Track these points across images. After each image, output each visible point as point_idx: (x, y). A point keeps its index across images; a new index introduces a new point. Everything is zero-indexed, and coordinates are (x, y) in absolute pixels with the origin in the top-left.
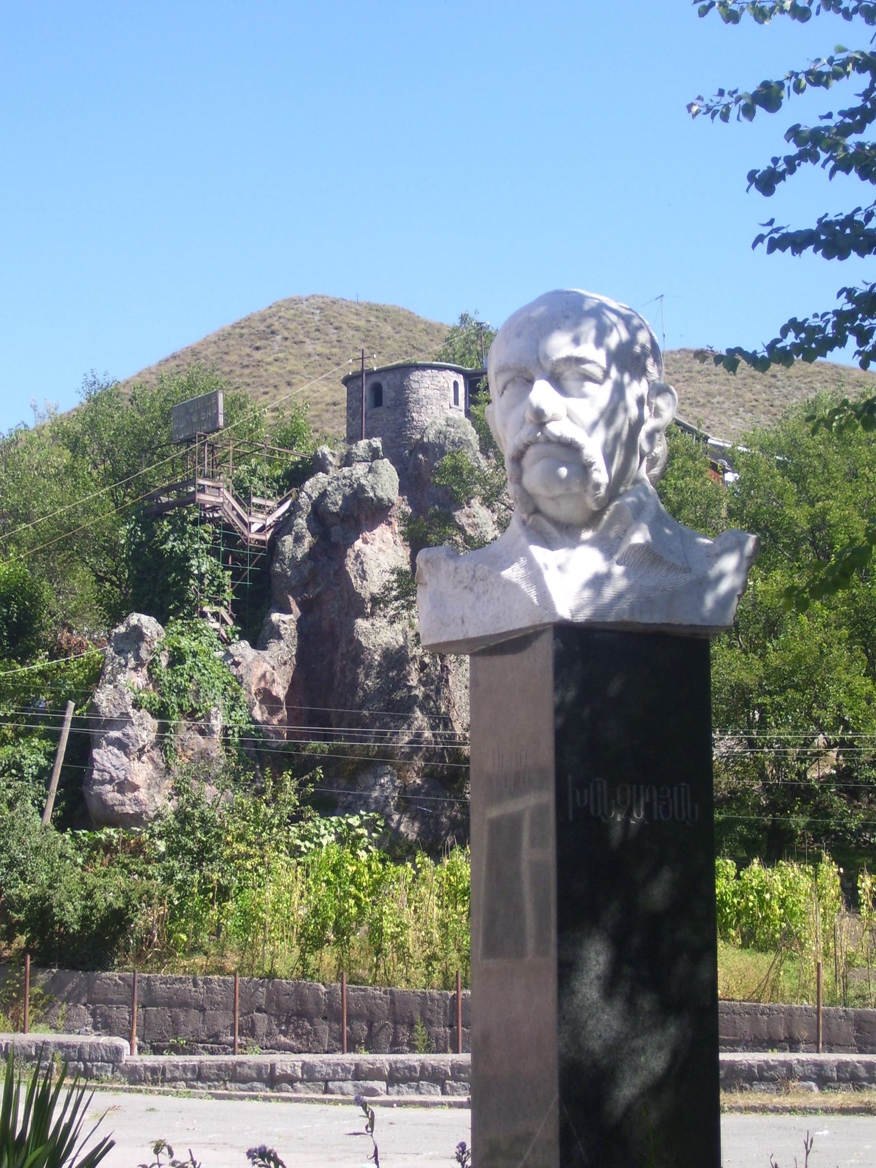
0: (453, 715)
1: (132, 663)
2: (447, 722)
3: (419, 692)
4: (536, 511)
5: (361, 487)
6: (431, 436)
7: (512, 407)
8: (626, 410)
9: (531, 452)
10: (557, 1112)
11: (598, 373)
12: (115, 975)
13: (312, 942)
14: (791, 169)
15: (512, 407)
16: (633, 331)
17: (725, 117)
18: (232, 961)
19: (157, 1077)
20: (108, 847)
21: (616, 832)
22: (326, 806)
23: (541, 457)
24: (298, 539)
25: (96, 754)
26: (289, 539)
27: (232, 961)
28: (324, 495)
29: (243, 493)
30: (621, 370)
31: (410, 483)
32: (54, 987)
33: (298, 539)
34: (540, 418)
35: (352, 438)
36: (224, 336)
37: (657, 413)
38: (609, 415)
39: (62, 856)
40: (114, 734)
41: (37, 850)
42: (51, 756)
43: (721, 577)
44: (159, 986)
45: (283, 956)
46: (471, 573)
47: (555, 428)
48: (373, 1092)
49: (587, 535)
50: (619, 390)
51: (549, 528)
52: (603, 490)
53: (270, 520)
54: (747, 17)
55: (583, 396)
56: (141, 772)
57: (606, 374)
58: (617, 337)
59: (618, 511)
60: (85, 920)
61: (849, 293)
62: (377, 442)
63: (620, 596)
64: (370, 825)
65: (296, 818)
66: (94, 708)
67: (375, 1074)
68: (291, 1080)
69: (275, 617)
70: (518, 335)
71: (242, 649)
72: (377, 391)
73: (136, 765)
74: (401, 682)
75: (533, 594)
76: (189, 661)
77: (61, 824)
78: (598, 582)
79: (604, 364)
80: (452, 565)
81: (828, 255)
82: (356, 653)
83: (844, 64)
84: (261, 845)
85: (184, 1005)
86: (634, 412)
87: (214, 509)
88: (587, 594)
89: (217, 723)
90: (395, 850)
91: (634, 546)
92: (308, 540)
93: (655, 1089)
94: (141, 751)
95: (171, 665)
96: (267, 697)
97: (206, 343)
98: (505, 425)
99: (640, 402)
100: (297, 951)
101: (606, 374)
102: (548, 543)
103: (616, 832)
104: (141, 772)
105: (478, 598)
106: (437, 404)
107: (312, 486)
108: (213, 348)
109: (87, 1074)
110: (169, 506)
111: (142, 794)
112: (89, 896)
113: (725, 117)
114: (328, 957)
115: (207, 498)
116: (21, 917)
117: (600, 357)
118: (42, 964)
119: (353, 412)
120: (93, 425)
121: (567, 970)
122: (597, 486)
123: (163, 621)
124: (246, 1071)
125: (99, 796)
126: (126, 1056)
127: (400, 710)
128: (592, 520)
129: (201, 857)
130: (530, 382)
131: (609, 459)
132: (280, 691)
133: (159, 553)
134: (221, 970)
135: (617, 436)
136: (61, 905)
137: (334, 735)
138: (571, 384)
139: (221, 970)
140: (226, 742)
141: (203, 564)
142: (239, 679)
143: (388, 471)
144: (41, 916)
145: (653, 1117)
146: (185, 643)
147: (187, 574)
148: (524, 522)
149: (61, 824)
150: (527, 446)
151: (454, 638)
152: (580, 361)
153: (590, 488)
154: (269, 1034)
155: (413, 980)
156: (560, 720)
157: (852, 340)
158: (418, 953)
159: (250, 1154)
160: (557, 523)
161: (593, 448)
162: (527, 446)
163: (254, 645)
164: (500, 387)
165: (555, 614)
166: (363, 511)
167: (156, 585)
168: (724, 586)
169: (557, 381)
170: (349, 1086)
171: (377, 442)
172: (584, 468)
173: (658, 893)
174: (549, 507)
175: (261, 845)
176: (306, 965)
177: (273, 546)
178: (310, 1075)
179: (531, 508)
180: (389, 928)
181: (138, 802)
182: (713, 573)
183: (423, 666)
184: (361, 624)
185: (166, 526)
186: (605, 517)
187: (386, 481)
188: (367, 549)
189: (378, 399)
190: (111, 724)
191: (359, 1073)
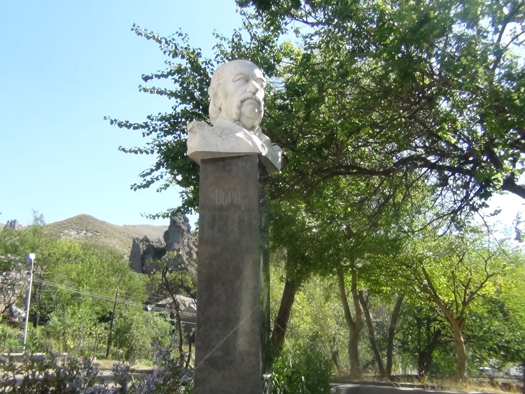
9: (249, 101)
46: (221, 132)
75: (250, 143)
105: (223, 140)
150: (248, 99)
151: (213, 151)
162: (248, 99)
174: (244, 120)
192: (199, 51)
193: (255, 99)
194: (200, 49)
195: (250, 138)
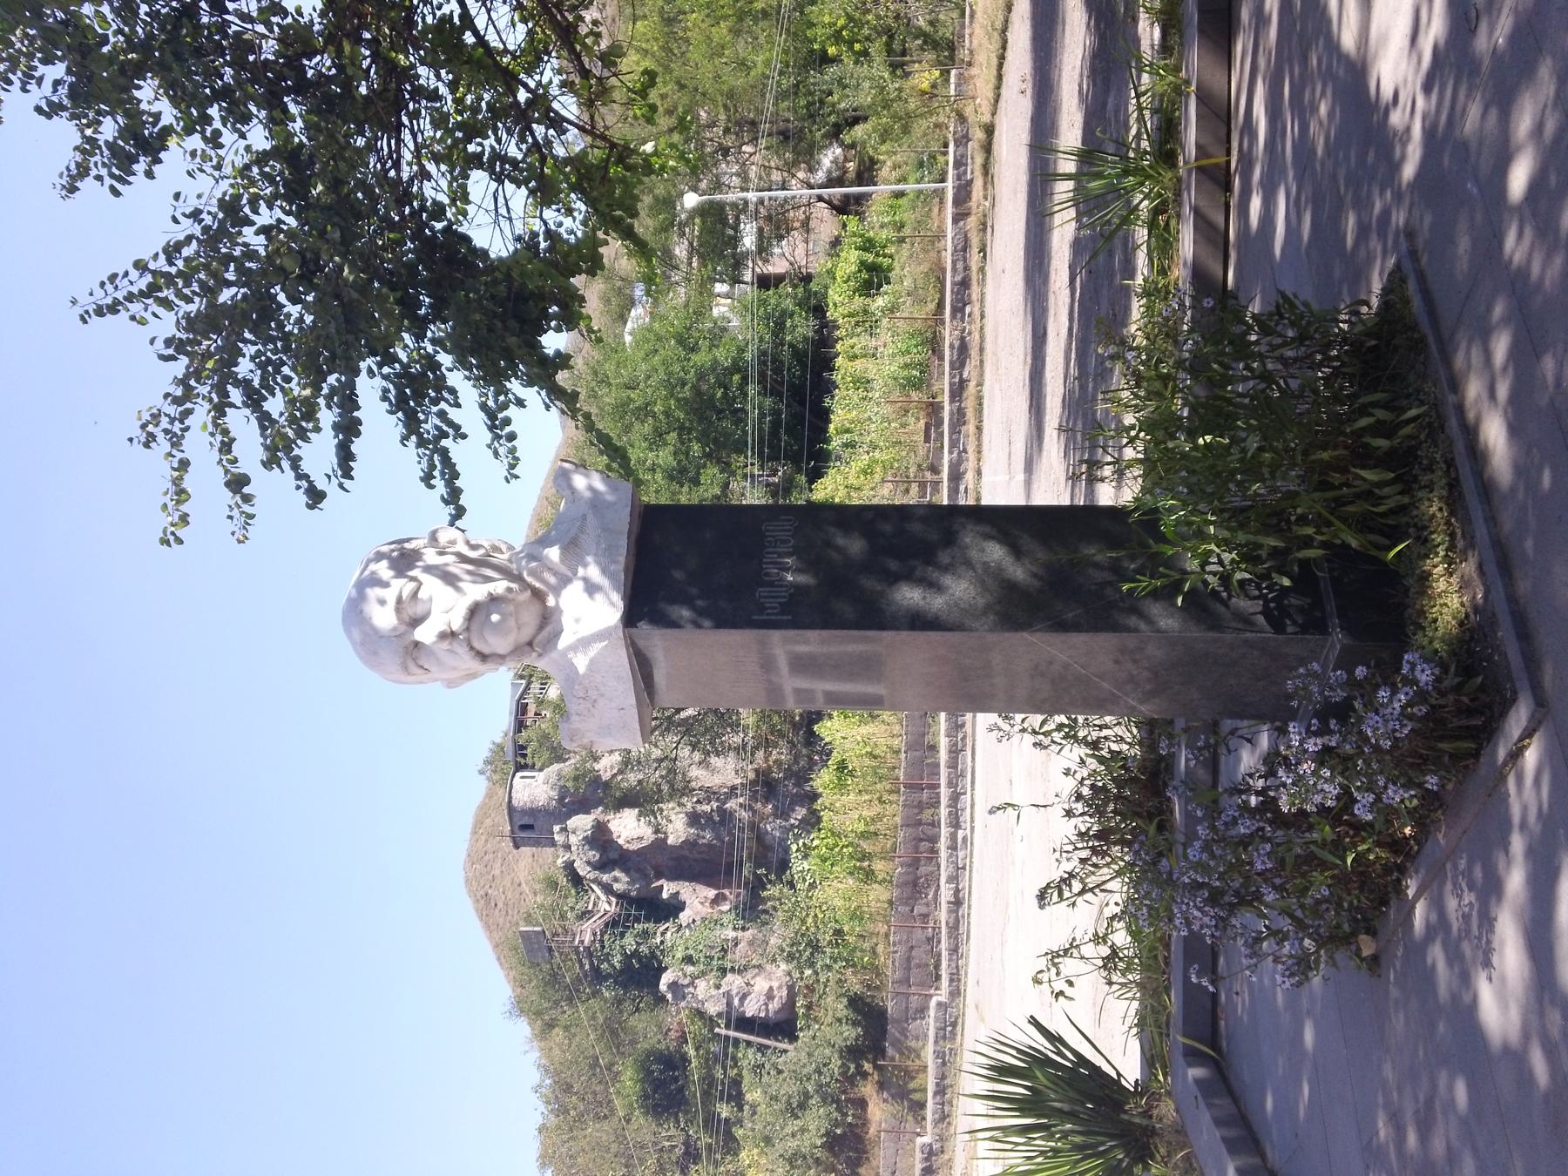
0: (730, 784)
1: (691, 989)
2: (733, 788)
3: (715, 805)
4: (530, 644)
5: (585, 838)
6: (554, 794)
7: (439, 661)
9: (477, 645)
10: (1039, 635)
11: (413, 585)
12: (890, 1005)
13: (869, 875)
14: (306, 477)
15: (439, 661)
16: (379, 556)
17: (252, 517)
18: (882, 928)
19: (955, 978)
20: (809, 1007)
21: (803, 579)
22: (784, 865)
23: (482, 637)
24: (616, 880)
25: (749, 1014)
26: (616, 886)
27: (882, 928)
28: (588, 863)
29: (585, 915)
30: (411, 567)
31: (583, 806)
32: (897, 1044)
33: (616, 880)
34: (448, 635)
35: (553, 844)
36: (487, 926)
37: (453, 542)
38: (450, 579)
39: (814, 1038)
40: (736, 1002)
41: (810, 1055)
42: (749, 1044)
43: (591, 488)
44: (898, 975)
45: (878, 895)
47: (457, 623)
48: (965, 839)
49: (551, 601)
51: (545, 633)
52: (514, 586)
53: (603, 897)
54: (184, 508)
55: (431, 599)
56: (761, 985)
57: (413, 579)
58: (383, 570)
59: (532, 573)
60: (855, 1024)
61: (404, 439)
62: (557, 828)
63: (604, 571)
64: (797, 837)
65: (792, 885)
66: (719, 1015)
67: (953, 837)
68: (957, 891)
69: (665, 895)
70: (375, 653)
71: (684, 917)
72: (524, 827)
73: (756, 988)
74: (708, 816)
75: (599, 646)
76: (691, 952)
77: (793, 1038)
78: (591, 588)
79: (404, 581)
80: (574, 718)
81: (358, 434)
82: (689, 844)
83: (216, 425)
84: (809, 908)
85: (909, 959)
86: (450, 559)
87: (595, 934)
88: (599, 597)
89: (731, 934)
90: (812, 822)
91: (562, 561)
92: (617, 873)
93: (1017, 552)
94: (748, 984)
95: (693, 964)
96: (716, 901)
97: (490, 938)
98: (455, 668)
99: (441, 554)
100: (875, 886)
101: (413, 579)
102: (558, 634)
103: (803, 579)
104: (761, 985)
106: (535, 789)
107: (583, 870)
108: (495, 934)
109: (954, 1024)
110: (592, 963)
111: (775, 985)
112: (839, 1020)
113: (252, 517)
114: (879, 866)
115: (587, 939)
116: (852, 1067)
118: (882, 1052)
119: (537, 843)
120: (538, 1014)
121: (920, 622)
122: (509, 590)
123: (666, 968)
124: (952, 920)
125: (776, 1013)
126: (943, 999)
127: (726, 817)
128: (538, 596)
129: (815, 947)
130: (417, 644)
131: (488, 579)
132: (712, 893)
133: (622, 972)
134: (887, 935)
135: (469, 572)
136: (845, 1040)
137: (740, 861)
138: (420, 609)
139: (887, 935)
140: (743, 929)
141: (629, 942)
142: (704, 919)
143: (573, 822)
144: (853, 1053)
145: (1042, 554)
146: (679, 955)
147: (635, 954)
148: (540, 655)
149: (793, 1038)
150: (472, 648)
152: (399, 601)
153: (510, 596)
154: (927, 905)
155: (895, 812)
156: (707, 623)
157: (444, 443)
158: (877, 809)
159: (1042, 907)
160: (541, 627)
161: (477, 592)
162: (472, 648)
163: (683, 909)
164: (420, 671)
165: (616, 627)
166: (600, 838)
167: (641, 975)
168: (599, 485)
169: (416, 622)
170: (961, 854)
171: (557, 828)
172: (493, 599)
173: (855, 546)
174: (527, 633)
175: (809, 908)
176: (884, 880)
177: (620, 896)
178: (954, 879)
179: (528, 648)
180: (861, 827)
181: (780, 987)
182: (588, 494)
183: (699, 802)
184: (669, 842)
185: (604, 966)
186: (538, 585)
187: (582, 823)
188: (623, 836)
189: (529, 827)
190: (729, 1004)
191: (953, 847)
192: (159, 344)
193: (468, 629)
194: (152, 342)
195: (583, 643)
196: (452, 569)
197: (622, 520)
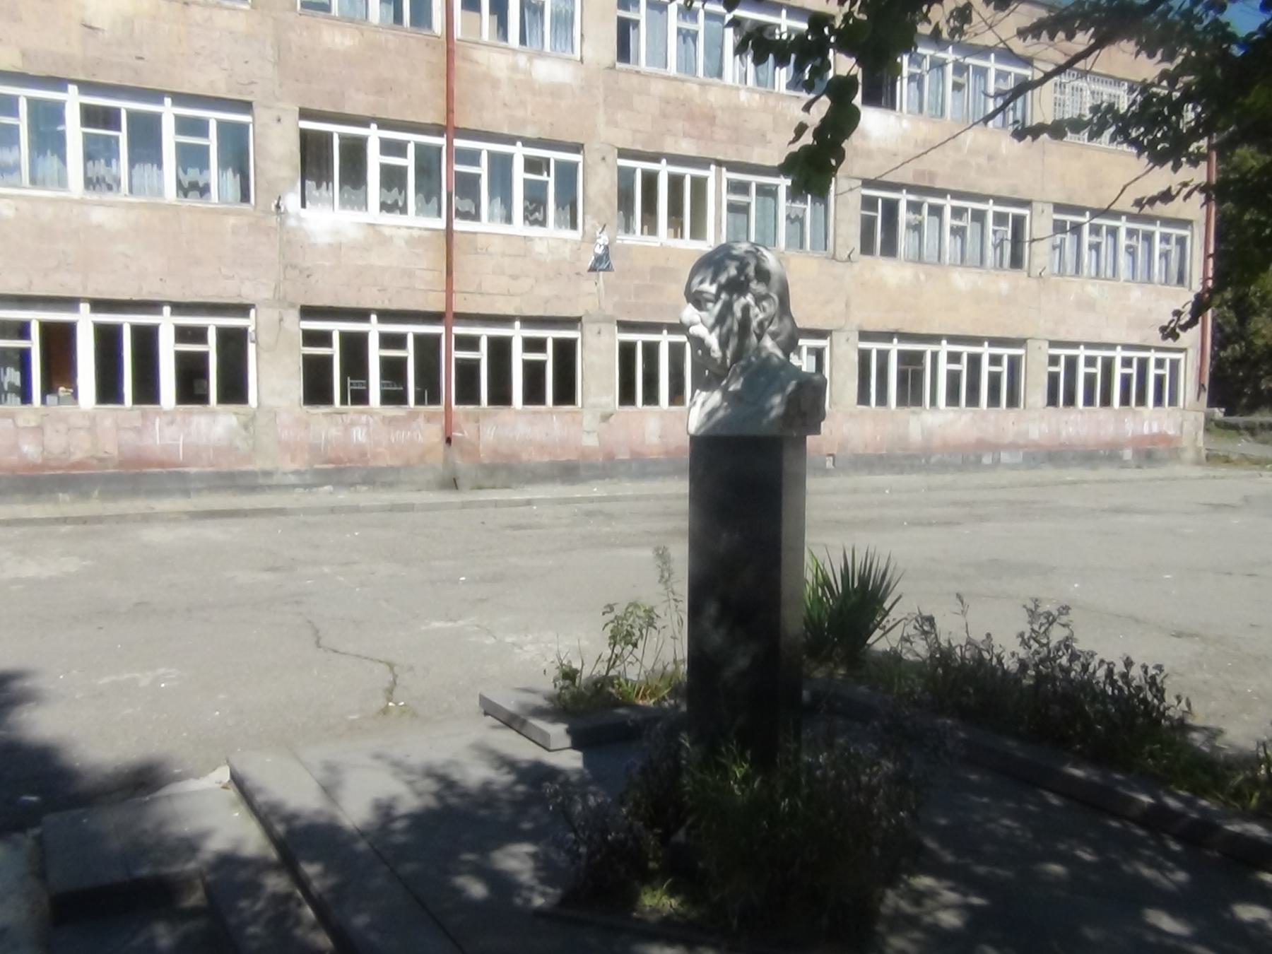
8: (733, 314)
11: (712, 298)
30: (730, 293)
38: (720, 320)
43: (772, 408)
50: (728, 307)
55: (707, 310)
86: (738, 314)
117: (713, 289)
122: (715, 360)
131: (723, 344)
161: (712, 340)
168: (774, 414)
196: (729, 322)
197: (749, 430)
